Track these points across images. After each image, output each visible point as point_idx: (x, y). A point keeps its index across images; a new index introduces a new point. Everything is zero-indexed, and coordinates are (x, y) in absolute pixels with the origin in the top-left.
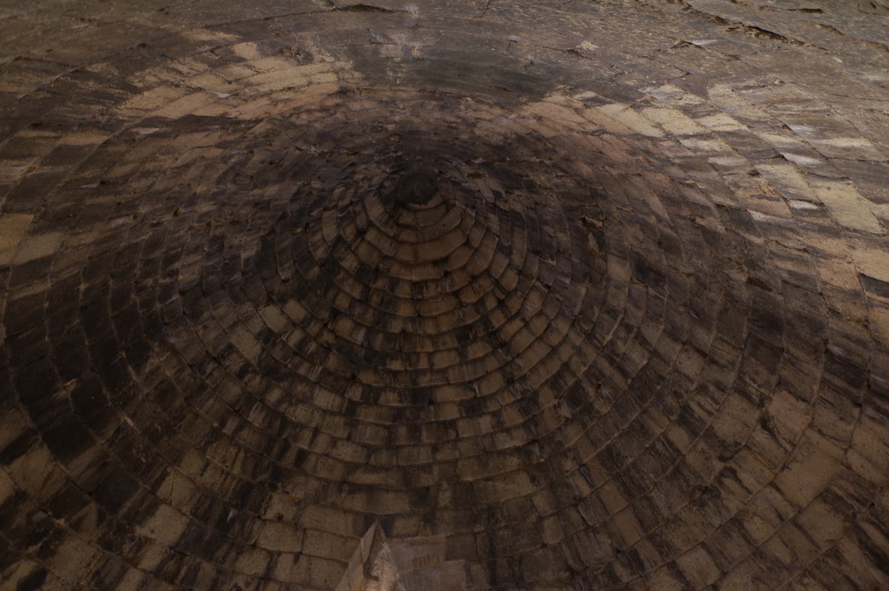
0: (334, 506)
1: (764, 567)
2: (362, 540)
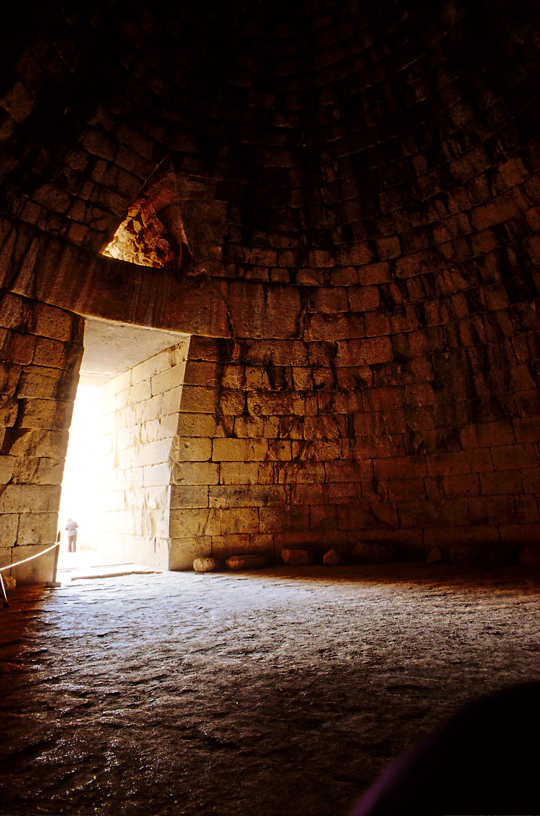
1: (431, 257)
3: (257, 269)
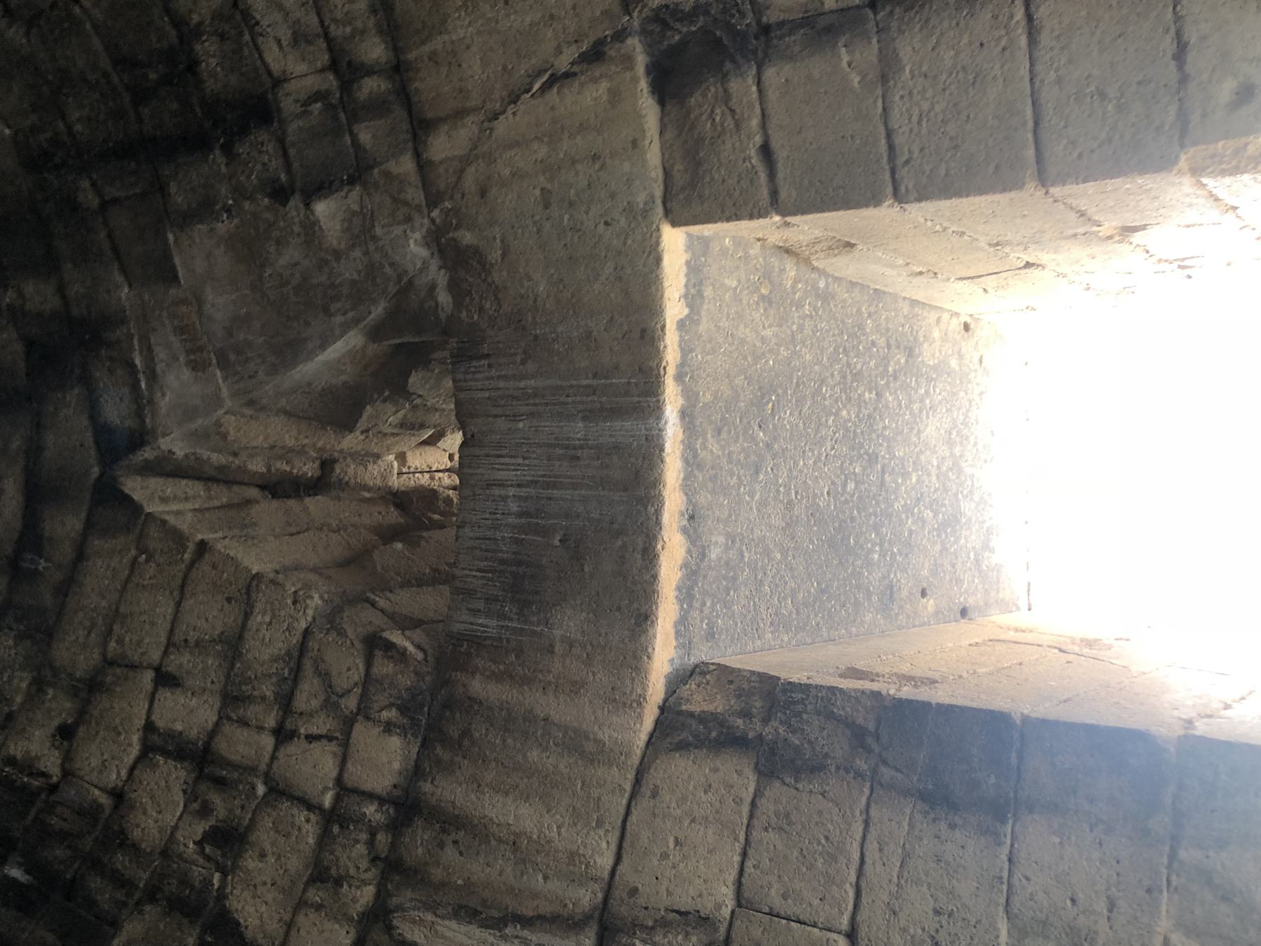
0: (66, 587)
2: (148, 510)
3: (335, 20)
